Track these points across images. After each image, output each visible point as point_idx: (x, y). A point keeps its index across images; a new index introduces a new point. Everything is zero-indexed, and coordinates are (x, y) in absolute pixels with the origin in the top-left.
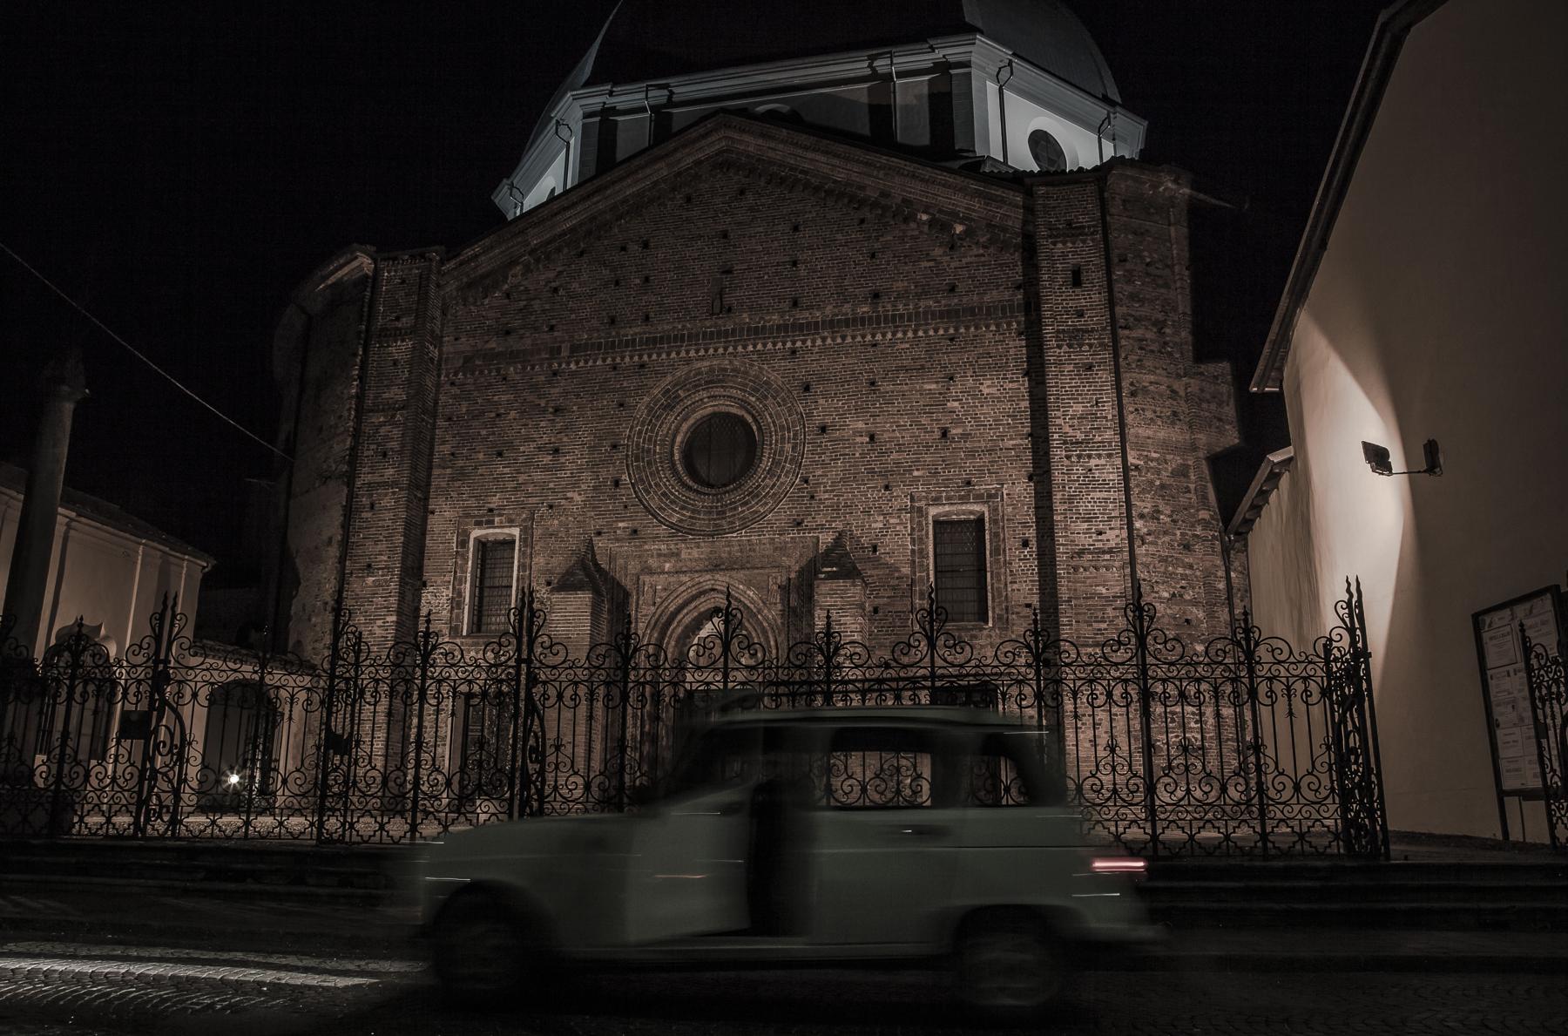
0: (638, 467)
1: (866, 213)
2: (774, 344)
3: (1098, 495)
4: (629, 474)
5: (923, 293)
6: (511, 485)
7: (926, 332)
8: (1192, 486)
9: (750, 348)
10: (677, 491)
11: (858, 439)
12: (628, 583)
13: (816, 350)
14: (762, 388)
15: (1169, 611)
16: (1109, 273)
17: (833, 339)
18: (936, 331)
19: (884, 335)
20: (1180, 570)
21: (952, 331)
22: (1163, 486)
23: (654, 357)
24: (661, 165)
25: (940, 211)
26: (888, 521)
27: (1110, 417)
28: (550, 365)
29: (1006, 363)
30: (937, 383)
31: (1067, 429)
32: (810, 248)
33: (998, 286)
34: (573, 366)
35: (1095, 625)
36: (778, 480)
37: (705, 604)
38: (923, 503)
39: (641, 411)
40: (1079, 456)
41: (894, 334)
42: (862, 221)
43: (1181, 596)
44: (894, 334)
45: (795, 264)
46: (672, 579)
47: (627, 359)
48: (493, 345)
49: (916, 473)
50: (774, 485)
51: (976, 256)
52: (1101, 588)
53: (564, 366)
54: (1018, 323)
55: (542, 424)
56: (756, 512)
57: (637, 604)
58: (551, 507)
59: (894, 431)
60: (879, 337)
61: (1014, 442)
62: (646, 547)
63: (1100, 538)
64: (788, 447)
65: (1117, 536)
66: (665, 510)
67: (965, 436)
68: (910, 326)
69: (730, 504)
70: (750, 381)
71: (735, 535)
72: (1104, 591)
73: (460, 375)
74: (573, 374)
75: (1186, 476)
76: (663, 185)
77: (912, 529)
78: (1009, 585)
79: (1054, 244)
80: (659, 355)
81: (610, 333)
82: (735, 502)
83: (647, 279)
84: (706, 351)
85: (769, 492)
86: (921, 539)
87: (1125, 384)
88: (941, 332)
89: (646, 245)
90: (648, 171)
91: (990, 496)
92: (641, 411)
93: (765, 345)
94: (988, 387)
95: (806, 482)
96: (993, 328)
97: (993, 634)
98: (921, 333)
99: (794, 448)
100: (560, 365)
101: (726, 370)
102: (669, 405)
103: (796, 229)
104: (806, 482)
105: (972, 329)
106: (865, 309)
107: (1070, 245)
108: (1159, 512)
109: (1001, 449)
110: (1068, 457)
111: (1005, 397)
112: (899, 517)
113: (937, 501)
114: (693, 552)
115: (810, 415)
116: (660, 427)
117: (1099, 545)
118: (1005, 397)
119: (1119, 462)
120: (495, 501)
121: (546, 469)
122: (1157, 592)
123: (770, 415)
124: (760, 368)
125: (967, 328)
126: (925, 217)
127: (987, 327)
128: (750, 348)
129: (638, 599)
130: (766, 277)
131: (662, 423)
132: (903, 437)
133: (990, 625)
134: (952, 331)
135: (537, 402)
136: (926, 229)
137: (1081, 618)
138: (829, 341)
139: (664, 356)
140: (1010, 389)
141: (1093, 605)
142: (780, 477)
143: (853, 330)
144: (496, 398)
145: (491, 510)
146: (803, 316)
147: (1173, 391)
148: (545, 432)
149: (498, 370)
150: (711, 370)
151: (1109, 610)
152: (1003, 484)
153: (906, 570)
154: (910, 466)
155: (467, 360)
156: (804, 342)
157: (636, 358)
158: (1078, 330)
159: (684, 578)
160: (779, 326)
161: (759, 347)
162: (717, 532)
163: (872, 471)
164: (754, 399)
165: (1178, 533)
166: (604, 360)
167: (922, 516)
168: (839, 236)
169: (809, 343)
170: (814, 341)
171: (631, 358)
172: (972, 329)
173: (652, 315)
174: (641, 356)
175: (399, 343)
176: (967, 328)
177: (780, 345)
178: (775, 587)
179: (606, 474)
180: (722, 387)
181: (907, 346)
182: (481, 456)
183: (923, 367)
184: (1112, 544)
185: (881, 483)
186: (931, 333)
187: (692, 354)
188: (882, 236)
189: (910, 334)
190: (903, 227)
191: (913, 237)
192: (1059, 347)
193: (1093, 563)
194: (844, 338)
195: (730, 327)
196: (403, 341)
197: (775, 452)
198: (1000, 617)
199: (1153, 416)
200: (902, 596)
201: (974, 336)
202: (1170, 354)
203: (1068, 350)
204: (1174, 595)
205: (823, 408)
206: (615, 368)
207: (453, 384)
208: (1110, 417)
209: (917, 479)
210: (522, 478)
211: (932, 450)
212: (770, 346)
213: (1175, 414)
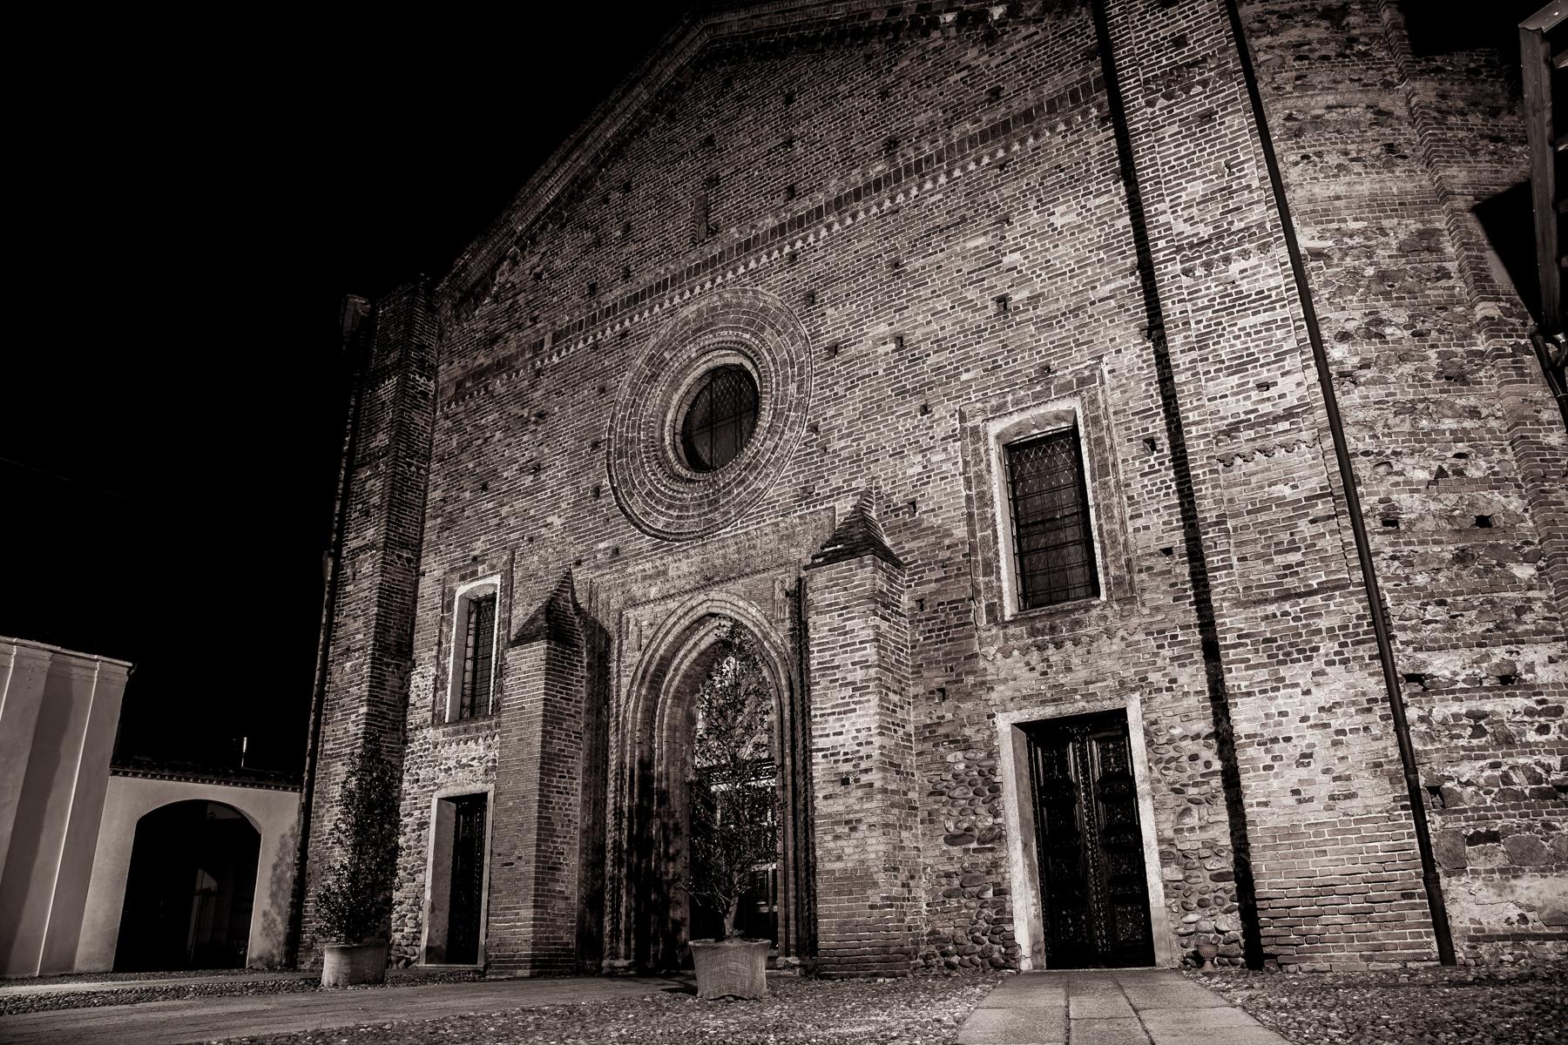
3: (1252, 320)
5: (956, 114)
6: (495, 521)
7: (964, 168)
8: (1452, 266)
10: (665, 486)
11: (881, 350)
12: (611, 626)
13: (821, 244)
14: (758, 319)
15: (1433, 506)
17: (841, 222)
18: (978, 161)
19: (907, 193)
20: (1449, 424)
22: (1382, 276)
23: (636, 319)
24: (640, 88)
26: (928, 460)
27: (1255, 184)
28: (533, 365)
29: (1086, 171)
30: (985, 234)
31: (1180, 226)
32: (808, 116)
33: (1061, 67)
34: (555, 359)
35: (1279, 560)
37: (706, 638)
39: (624, 393)
40: (1208, 265)
41: (920, 187)
42: (868, 58)
43: (1459, 473)
44: (920, 187)
45: (789, 143)
46: (658, 609)
48: (481, 360)
49: (964, 377)
50: (776, 447)
51: (1024, 39)
54: (1100, 107)
55: (525, 438)
56: (756, 491)
57: (620, 652)
59: (930, 322)
61: (1113, 286)
62: (630, 570)
63: (1266, 394)
64: (792, 388)
65: (1299, 384)
66: (649, 514)
67: (1034, 300)
68: (942, 167)
69: (724, 487)
70: (744, 313)
71: (728, 529)
72: (1287, 491)
73: (453, 406)
74: (555, 368)
75: (1436, 250)
77: (966, 463)
78: (1129, 523)
81: (591, 306)
82: (729, 484)
84: (692, 291)
86: (979, 477)
87: (1275, 122)
91: (1083, 382)
92: (624, 393)
94: (1063, 215)
96: (1062, 127)
97: (1108, 612)
98: (957, 173)
100: (542, 361)
101: (715, 309)
105: (1031, 140)
106: (879, 168)
108: (1380, 322)
109: (1093, 303)
110: (1186, 272)
111: (1090, 222)
112: (945, 450)
113: (999, 411)
114: (683, 566)
117: (1265, 408)
118: (1090, 222)
119: (1282, 252)
120: (479, 547)
122: (1401, 473)
124: (753, 291)
125: (1023, 142)
126: (950, 17)
127: (1052, 129)
129: (621, 644)
133: (1103, 597)
134: (1001, 154)
136: (953, 32)
137: (1247, 550)
138: (836, 227)
139: (646, 314)
140: (1096, 208)
141: (1269, 523)
142: (783, 432)
143: (865, 202)
144: (483, 421)
145: (475, 559)
146: (802, 206)
147: (1380, 113)
148: (527, 447)
149: (486, 388)
150: (699, 312)
151: (1303, 525)
153: (961, 532)
154: (957, 368)
155: (460, 385)
156: (804, 239)
158: (1179, 68)
159: (672, 605)
160: (773, 231)
161: (752, 265)
162: (710, 529)
163: (902, 392)
164: (748, 336)
165: (1432, 354)
168: (842, 88)
169: (811, 239)
170: (817, 234)
171: (612, 328)
172: (1031, 140)
176: (1023, 142)
178: (782, 596)
179: (586, 483)
180: (711, 332)
181: (940, 196)
182: (467, 494)
183: (963, 219)
184: (1291, 400)
185: (915, 404)
186: (972, 167)
187: (677, 300)
188: (896, 64)
189: (942, 180)
190: (923, 41)
191: (936, 50)
192: (1150, 104)
193: (1258, 444)
195: (717, 250)
197: (777, 399)
198: (1119, 582)
199: (1342, 160)
200: (957, 575)
202: (1364, 55)
203: (1166, 103)
204: (1441, 473)
205: (834, 319)
207: (447, 418)
208: (1255, 184)
211: (986, 335)
212: (764, 259)
213: (1390, 148)
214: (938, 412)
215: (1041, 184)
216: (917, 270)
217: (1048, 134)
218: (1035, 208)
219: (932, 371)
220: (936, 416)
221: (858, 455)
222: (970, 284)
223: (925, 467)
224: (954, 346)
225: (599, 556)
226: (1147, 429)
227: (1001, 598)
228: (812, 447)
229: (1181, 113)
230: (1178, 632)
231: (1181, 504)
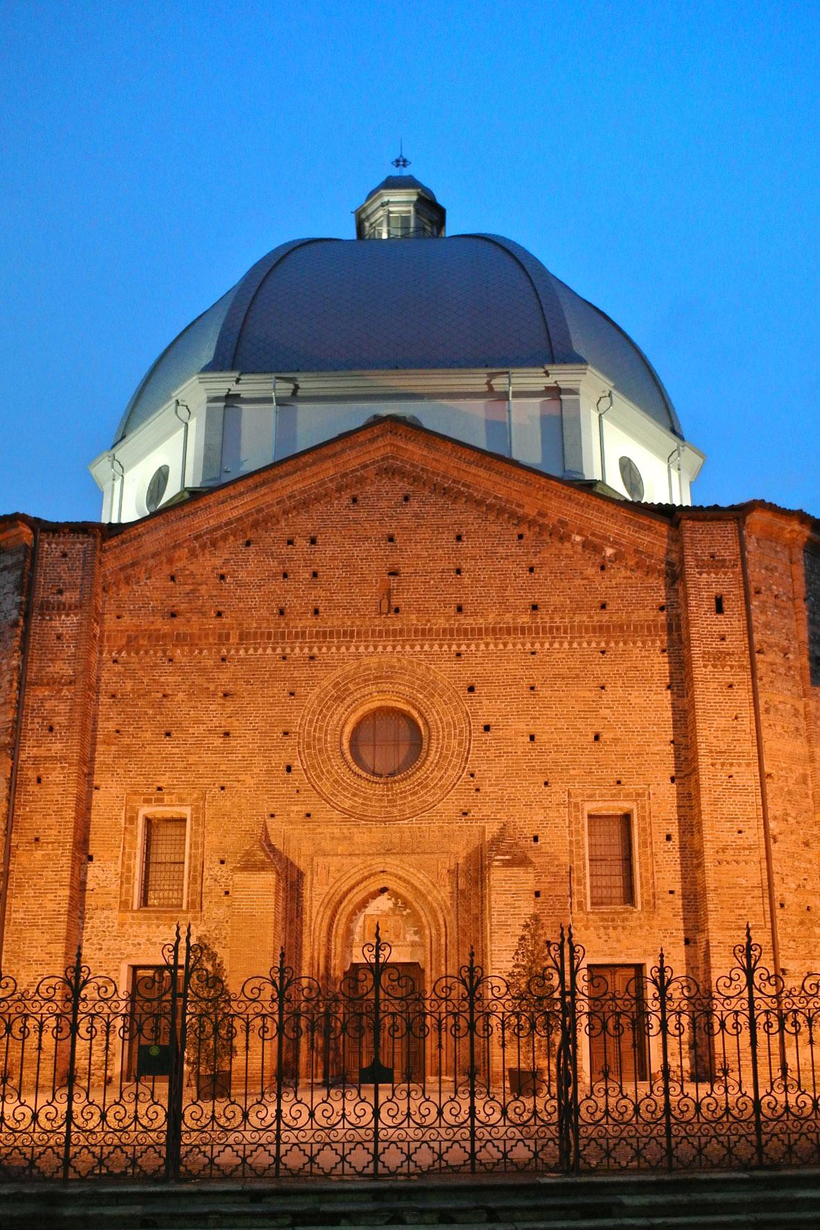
0: (309, 754)
1: (524, 529)
2: (441, 646)
3: (738, 798)
4: (301, 761)
5: (578, 609)
7: (580, 644)
8: (810, 792)
9: (418, 648)
10: (348, 778)
11: (521, 739)
12: (302, 864)
13: (480, 654)
14: (430, 687)
15: (796, 900)
16: (747, 603)
17: (496, 646)
18: (589, 644)
19: (542, 644)
20: (803, 865)
21: (603, 645)
22: (789, 793)
23: (324, 650)
25: (593, 534)
28: (219, 652)
29: (652, 677)
31: (712, 740)
32: (474, 558)
33: (644, 607)
34: (242, 652)
35: (737, 912)
36: (445, 773)
37: (375, 885)
38: (579, 799)
40: (723, 764)
41: (551, 644)
42: (521, 537)
43: (804, 887)
44: (551, 644)
45: (458, 571)
46: (344, 861)
47: (297, 650)
48: (158, 625)
49: (572, 772)
50: (442, 777)
51: (624, 578)
52: (741, 879)
53: (233, 652)
54: (662, 642)
55: (212, 707)
57: (312, 883)
58: (223, 788)
59: (552, 733)
60: (537, 646)
61: (659, 748)
62: (319, 830)
64: (454, 743)
65: (755, 835)
66: (337, 796)
67: (616, 741)
68: (566, 638)
69: (401, 793)
70: (418, 679)
71: (406, 822)
72: (744, 882)
73: (124, 654)
74: (241, 661)
75: (805, 783)
76: (330, 485)
77: (570, 822)
78: (655, 874)
79: (700, 573)
80: (329, 648)
81: (279, 624)
82: (405, 792)
83: (315, 575)
84: (376, 648)
85: (437, 784)
87: (761, 702)
88: (594, 645)
89: (313, 541)
90: (315, 469)
91: (638, 795)
93: (431, 646)
94: (636, 697)
95: (472, 775)
97: (641, 916)
98: (575, 645)
99: (460, 744)
100: (228, 651)
101: (394, 667)
102: (339, 697)
103: (459, 538)
104: (472, 775)
105: (621, 644)
106: (525, 620)
107: (713, 575)
108: (787, 814)
109: (648, 754)
110: (713, 765)
111: (650, 707)
113: (591, 797)
114: (363, 836)
115: (475, 714)
116: (331, 717)
117: (740, 842)
118: (650, 707)
119: (757, 769)
121: (216, 751)
122: (787, 884)
123: (437, 712)
124: (427, 667)
125: (617, 643)
126: (578, 538)
127: (635, 643)
128: (418, 648)
129: (312, 879)
130: (432, 582)
131: (333, 713)
132: (560, 739)
133: (639, 908)
134: (603, 645)
135: (206, 685)
136: (580, 548)
137: (724, 905)
138: (491, 647)
139: (334, 650)
140: (655, 700)
141: (736, 894)
142: (447, 769)
143: (515, 638)
144: (162, 679)
146: (467, 622)
147: (795, 709)
148: (215, 714)
149: (164, 651)
150: (380, 666)
151: (748, 898)
152: (649, 785)
153: (565, 859)
155: (130, 640)
156: (468, 646)
157: (306, 650)
158: (721, 652)
159: (356, 860)
160: (444, 630)
161: (426, 648)
162: (388, 819)
163: (532, 769)
164: (421, 696)
165: (801, 832)
166: (274, 649)
167: (578, 811)
168: (500, 549)
169: (473, 647)
170: (477, 646)
171: (301, 649)
172: (621, 644)
173: (321, 609)
174: (311, 649)
175: (63, 617)
176: (617, 643)
177: (445, 648)
178: (445, 871)
179: (280, 759)
180: (391, 683)
183: (577, 676)
185: (542, 779)
186: (585, 645)
187: (362, 649)
188: (540, 552)
189: (566, 645)
190: (559, 545)
191: (567, 556)
192: (705, 666)
193: (735, 858)
194: (505, 645)
195: (398, 626)
196: (67, 615)
198: (648, 903)
199: (782, 731)
200: (560, 882)
201: (623, 651)
202: (793, 677)
203: (712, 670)
204: (799, 886)
205: (487, 710)
206: (284, 658)
207: (115, 661)
208: (748, 731)
209: (573, 777)
210: (192, 759)
211: (587, 752)
212: (436, 647)
213: (797, 729)
214: (555, 788)
215: (625, 674)
216: (546, 698)
217: (631, 645)
218: (621, 687)
219: (553, 762)
220: (554, 790)
221: (502, 799)
222: (579, 718)
223: (545, 818)
224: (567, 752)
225: (292, 815)
226: (668, 829)
227: (586, 899)
228: (470, 785)
229: (719, 678)
230: (674, 931)
231: (681, 871)
